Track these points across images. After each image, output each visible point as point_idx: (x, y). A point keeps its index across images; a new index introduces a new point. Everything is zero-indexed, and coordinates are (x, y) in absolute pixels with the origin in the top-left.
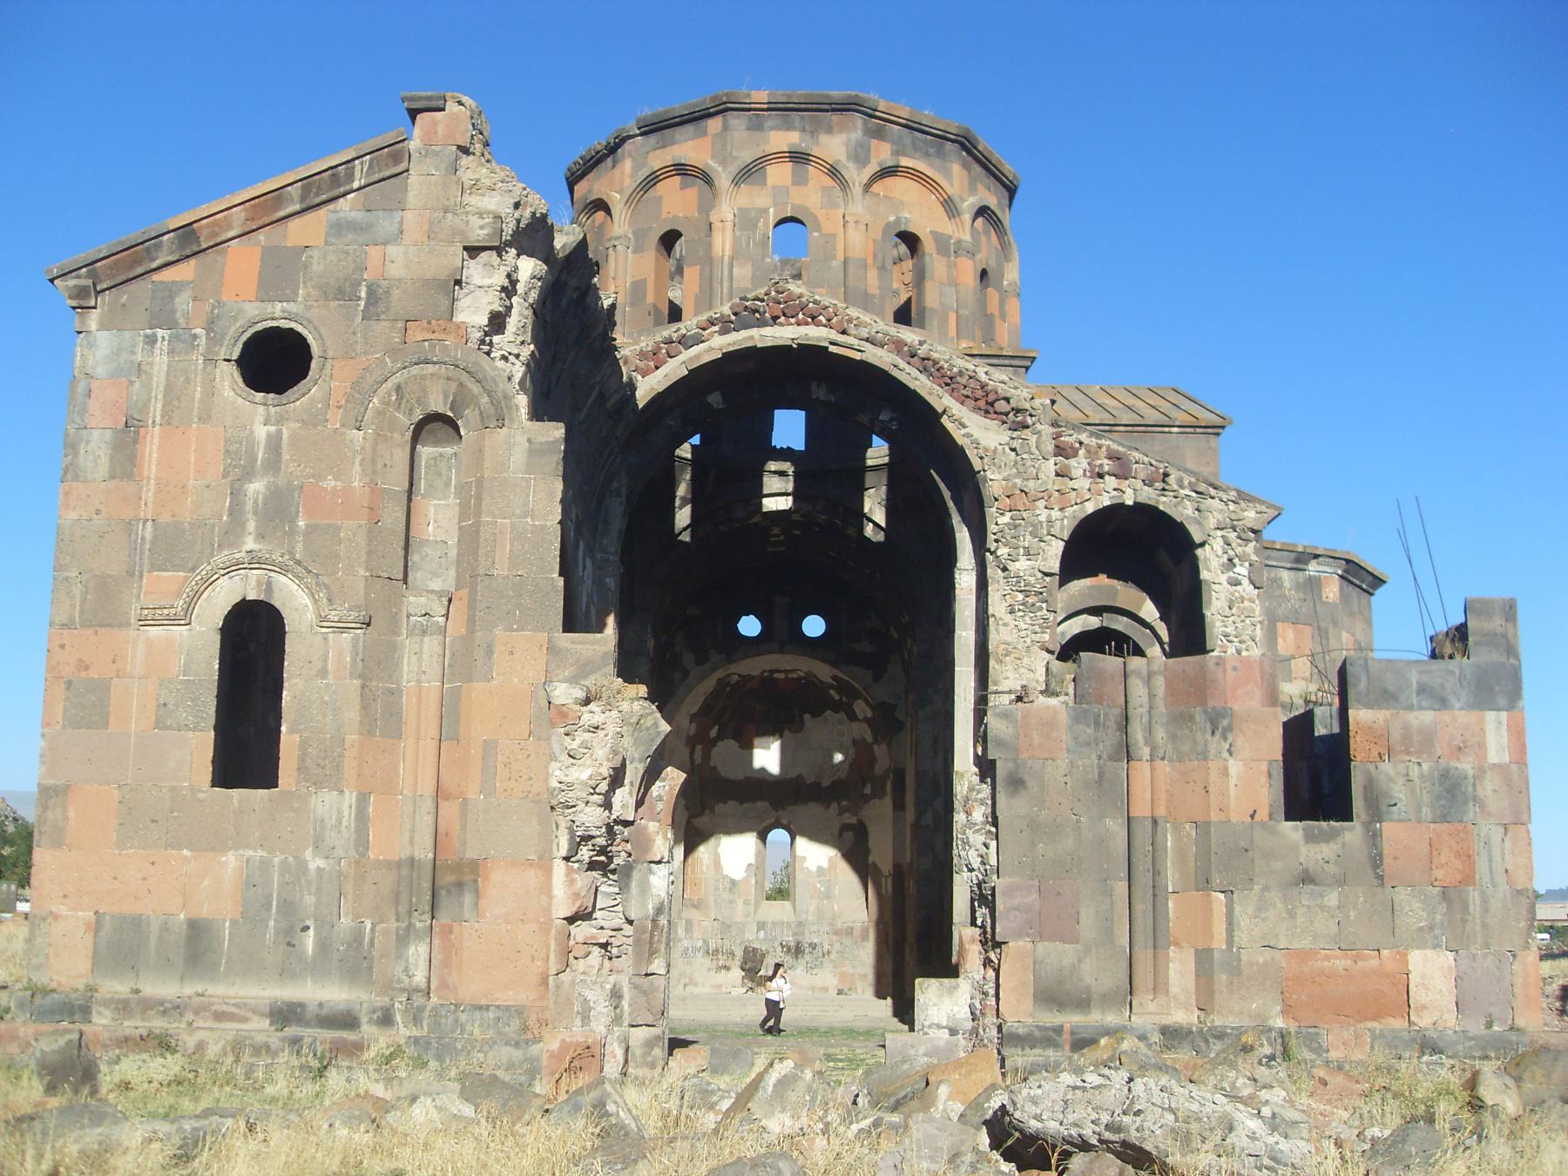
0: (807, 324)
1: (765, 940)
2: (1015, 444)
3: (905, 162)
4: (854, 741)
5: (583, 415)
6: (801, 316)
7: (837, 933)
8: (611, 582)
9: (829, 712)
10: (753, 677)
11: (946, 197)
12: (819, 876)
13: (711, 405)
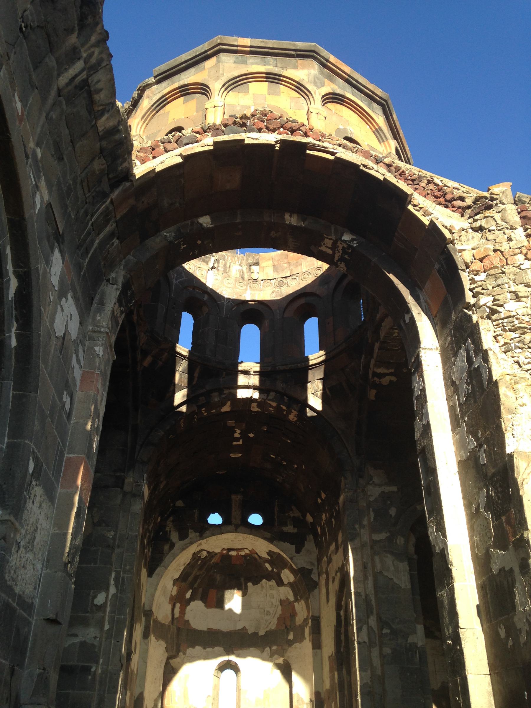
0: (288, 134)
2: (478, 224)
3: (349, 95)
4: (281, 601)
5: (63, 80)
6: (281, 130)
8: (99, 350)
9: (264, 580)
10: (216, 554)
11: (377, 127)
13: (201, 225)
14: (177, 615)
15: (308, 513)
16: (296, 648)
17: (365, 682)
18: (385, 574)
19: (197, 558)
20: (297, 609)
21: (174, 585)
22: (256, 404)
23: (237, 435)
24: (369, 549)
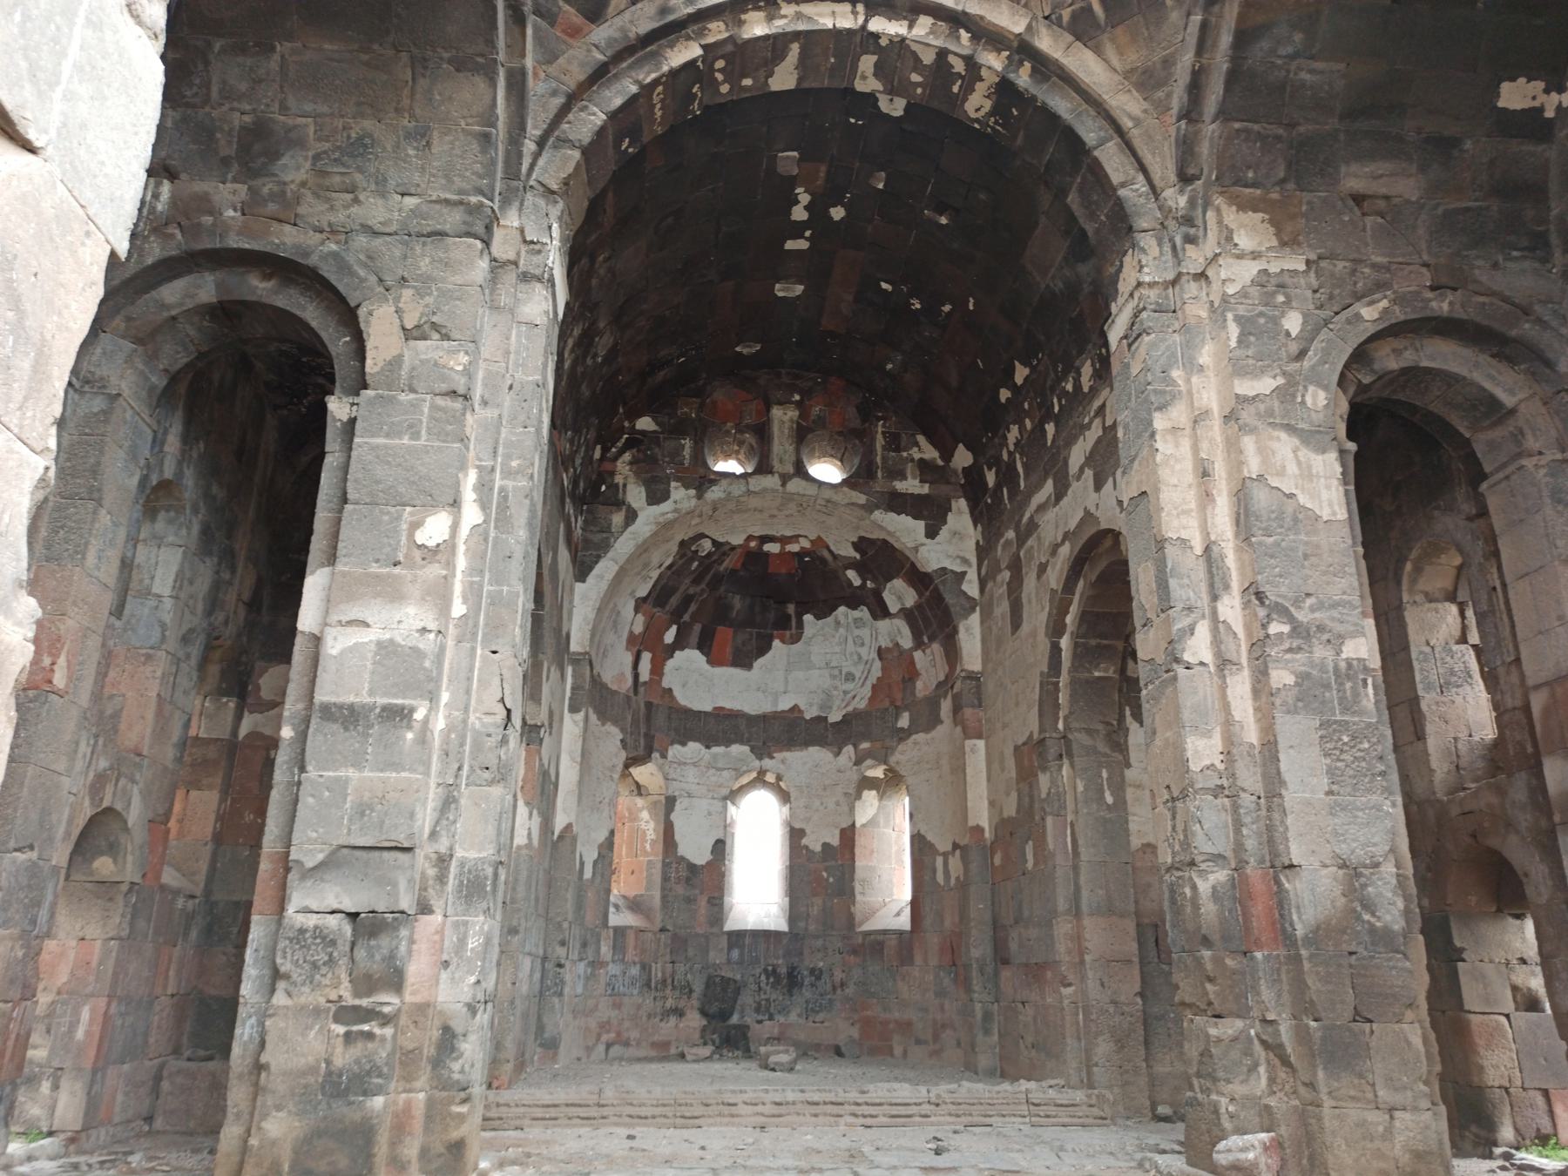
1: (741, 962)
4: (881, 652)
7: (854, 952)
9: (842, 609)
10: (733, 548)
12: (824, 860)
14: (645, 675)
15: (961, 446)
16: (915, 743)
17: (1208, 762)
18: (1274, 482)
19: (690, 554)
20: (918, 666)
21: (637, 610)
22: (874, 58)
23: (799, 214)
24: (1216, 428)
